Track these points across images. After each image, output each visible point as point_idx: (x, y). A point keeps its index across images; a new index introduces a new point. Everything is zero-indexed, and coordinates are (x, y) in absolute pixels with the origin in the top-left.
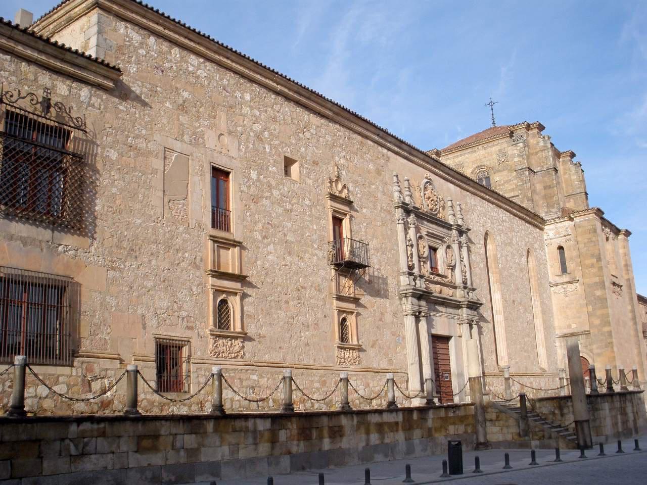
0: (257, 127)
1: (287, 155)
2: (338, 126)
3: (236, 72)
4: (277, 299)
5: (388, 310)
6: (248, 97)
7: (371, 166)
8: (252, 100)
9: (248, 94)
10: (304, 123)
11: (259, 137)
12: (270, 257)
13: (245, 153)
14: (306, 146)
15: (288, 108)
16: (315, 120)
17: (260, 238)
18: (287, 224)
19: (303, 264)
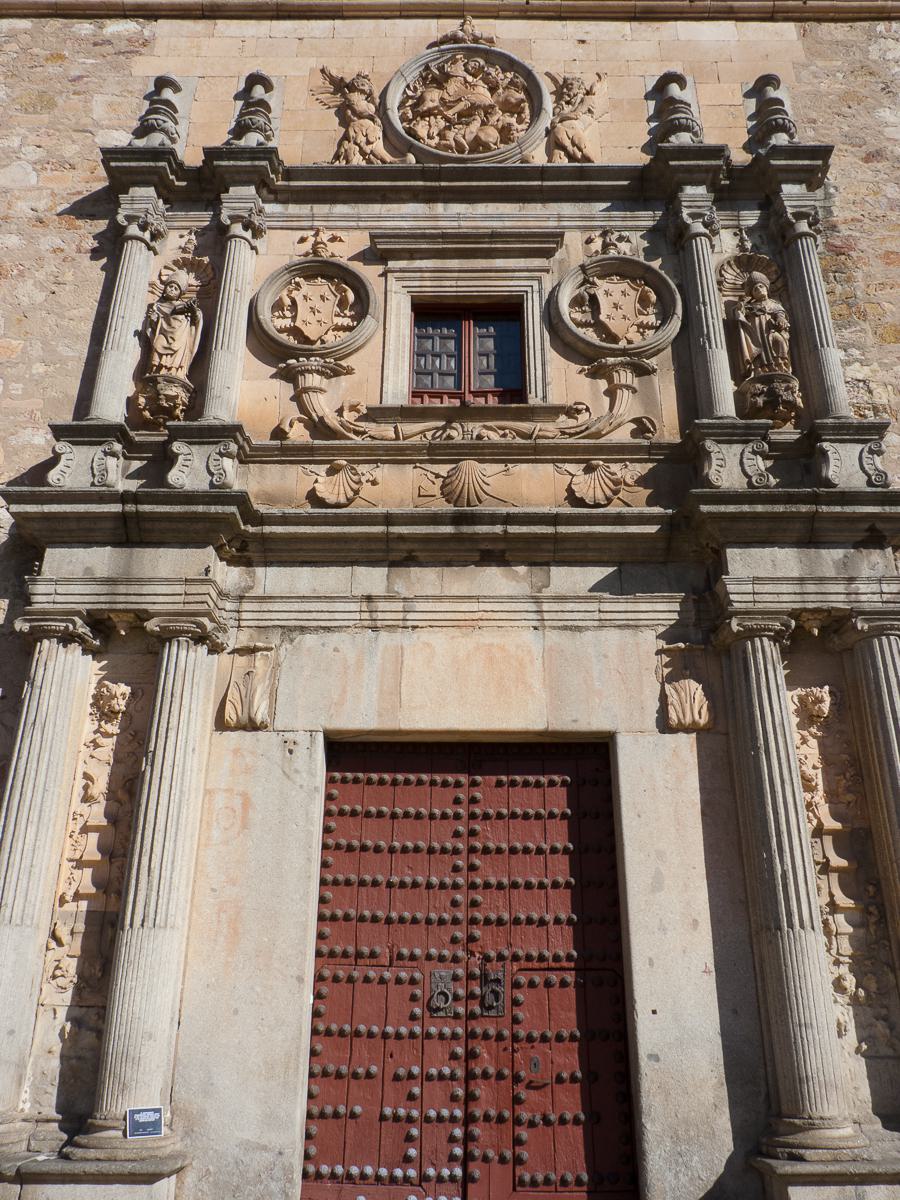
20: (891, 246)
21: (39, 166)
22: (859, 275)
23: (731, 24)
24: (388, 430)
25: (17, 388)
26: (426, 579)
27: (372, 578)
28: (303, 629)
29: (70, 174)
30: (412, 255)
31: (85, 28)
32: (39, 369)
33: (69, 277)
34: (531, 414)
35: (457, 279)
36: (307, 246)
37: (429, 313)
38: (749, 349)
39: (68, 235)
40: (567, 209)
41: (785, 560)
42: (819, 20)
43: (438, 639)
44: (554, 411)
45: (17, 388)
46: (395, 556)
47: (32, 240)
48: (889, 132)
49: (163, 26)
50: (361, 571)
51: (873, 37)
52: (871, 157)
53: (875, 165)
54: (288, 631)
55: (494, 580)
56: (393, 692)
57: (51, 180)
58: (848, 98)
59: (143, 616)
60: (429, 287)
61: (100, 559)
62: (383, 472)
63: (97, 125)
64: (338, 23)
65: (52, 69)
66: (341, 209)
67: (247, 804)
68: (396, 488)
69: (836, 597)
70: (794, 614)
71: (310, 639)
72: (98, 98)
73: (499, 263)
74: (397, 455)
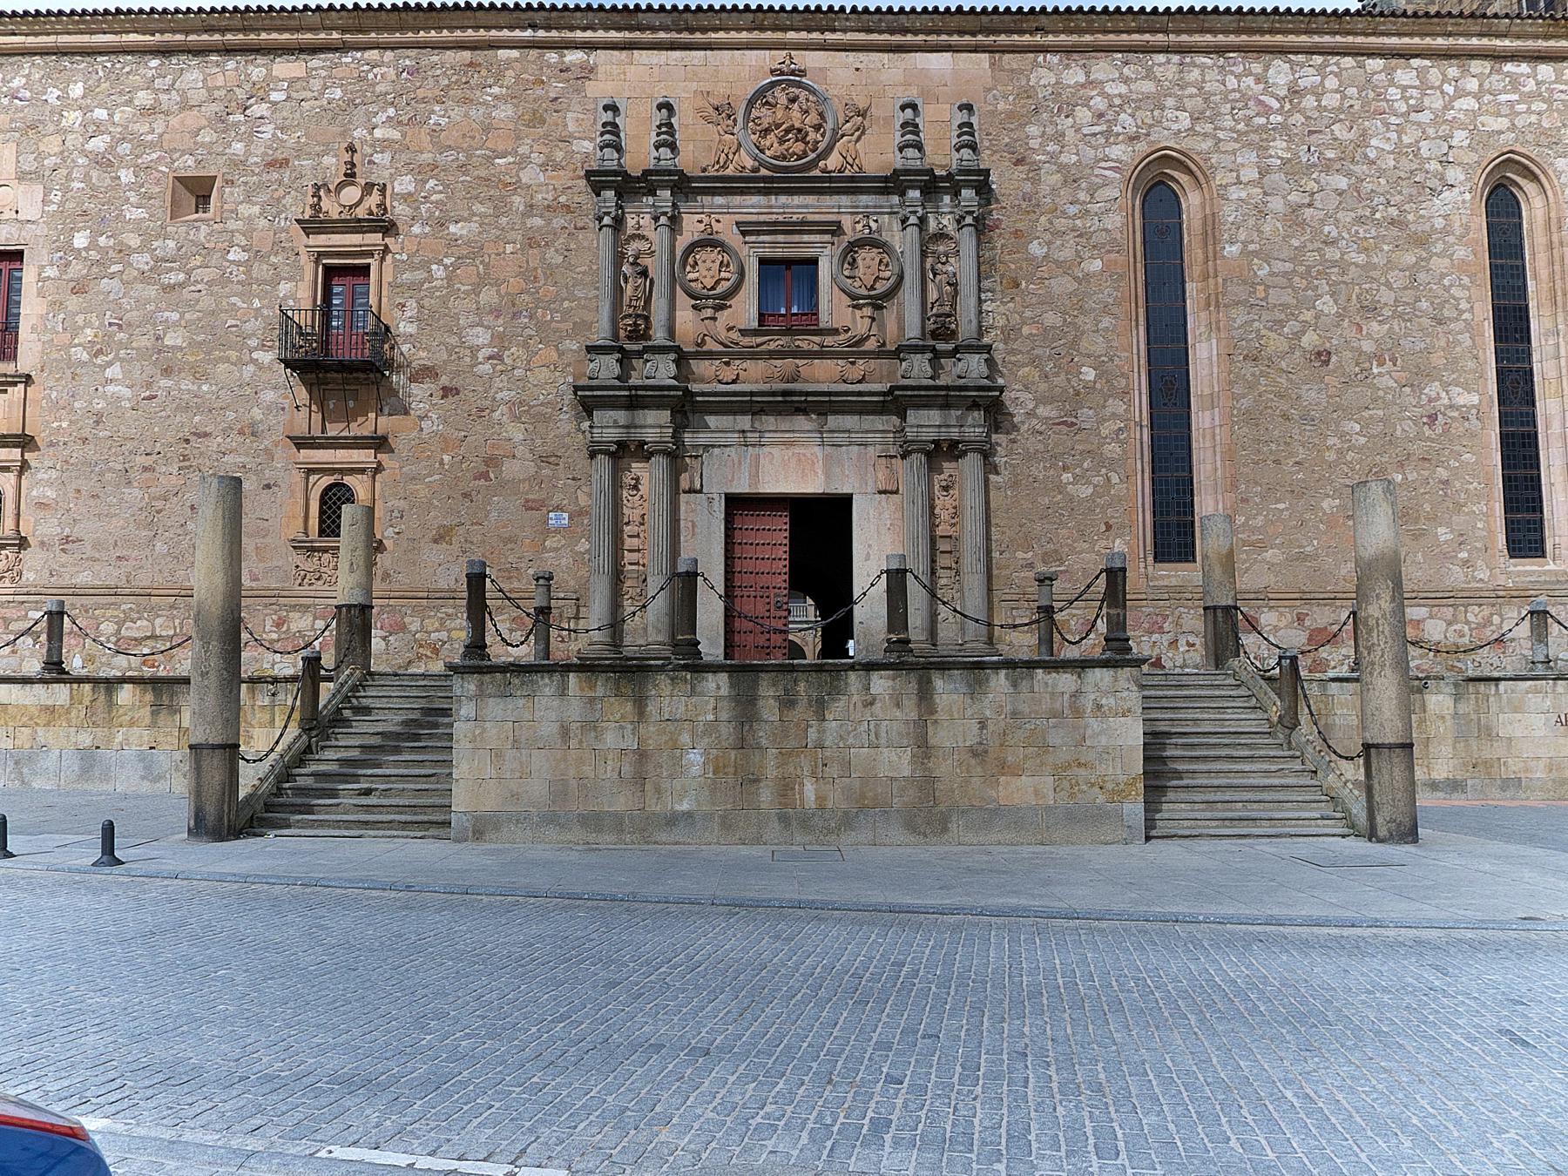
0: (98, 144)
1: (182, 173)
2: (373, 55)
3: (44, 52)
4: (120, 467)
5: (521, 451)
6: (77, 90)
7: (504, 112)
8: (88, 92)
9: (80, 84)
10: (247, 87)
11: (103, 162)
12: (111, 388)
13: (61, 204)
14: (250, 138)
15: (193, 75)
16: (286, 68)
17: (85, 356)
18: (167, 314)
19: (205, 388)
20: (1019, 226)
21: (543, 167)
22: (999, 245)
23: (949, 55)
24: (746, 341)
25: (558, 317)
26: (769, 421)
27: (744, 421)
28: (713, 446)
29: (562, 173)
30: (758, 233)
31: (552, 56)
32: (566, 304)
33: (573, 246)
34: (820, 332)
35: (780, 246)
36: (702, 227)
37: (763, 262)
38: (933, 295)
39: (568, 217)
40: (845, 200)
41: (934, 416)
42: (1003, 52)
43: (776, 451)
44: (835, 332)
45: (558, 317)
46: (755, 409)
47: (549, 222)
48: (1034, 144)
49: (601, 55)
50: (739, 418)
51: (1036, 65)
52: (1019, 162)
53: (1020, 168)
54: (706, 447)
55: (801, 422)
56: (755, 476)
57: (553, 178)
58: (1011, 115)
59: (642, 443)
60: (768, 253)
61: (621, 416)
62: (747, 364)
63: (571, 135)
64: (709, 53)
65: (539, 92)
66: (719, 200)
67: (694, 526)
68: (755, 376)
69: (954, 433)
70: (933, 442)
71: (716, 451)
72: (569, 115)
73: (806, 238)
74: (754, 355)
